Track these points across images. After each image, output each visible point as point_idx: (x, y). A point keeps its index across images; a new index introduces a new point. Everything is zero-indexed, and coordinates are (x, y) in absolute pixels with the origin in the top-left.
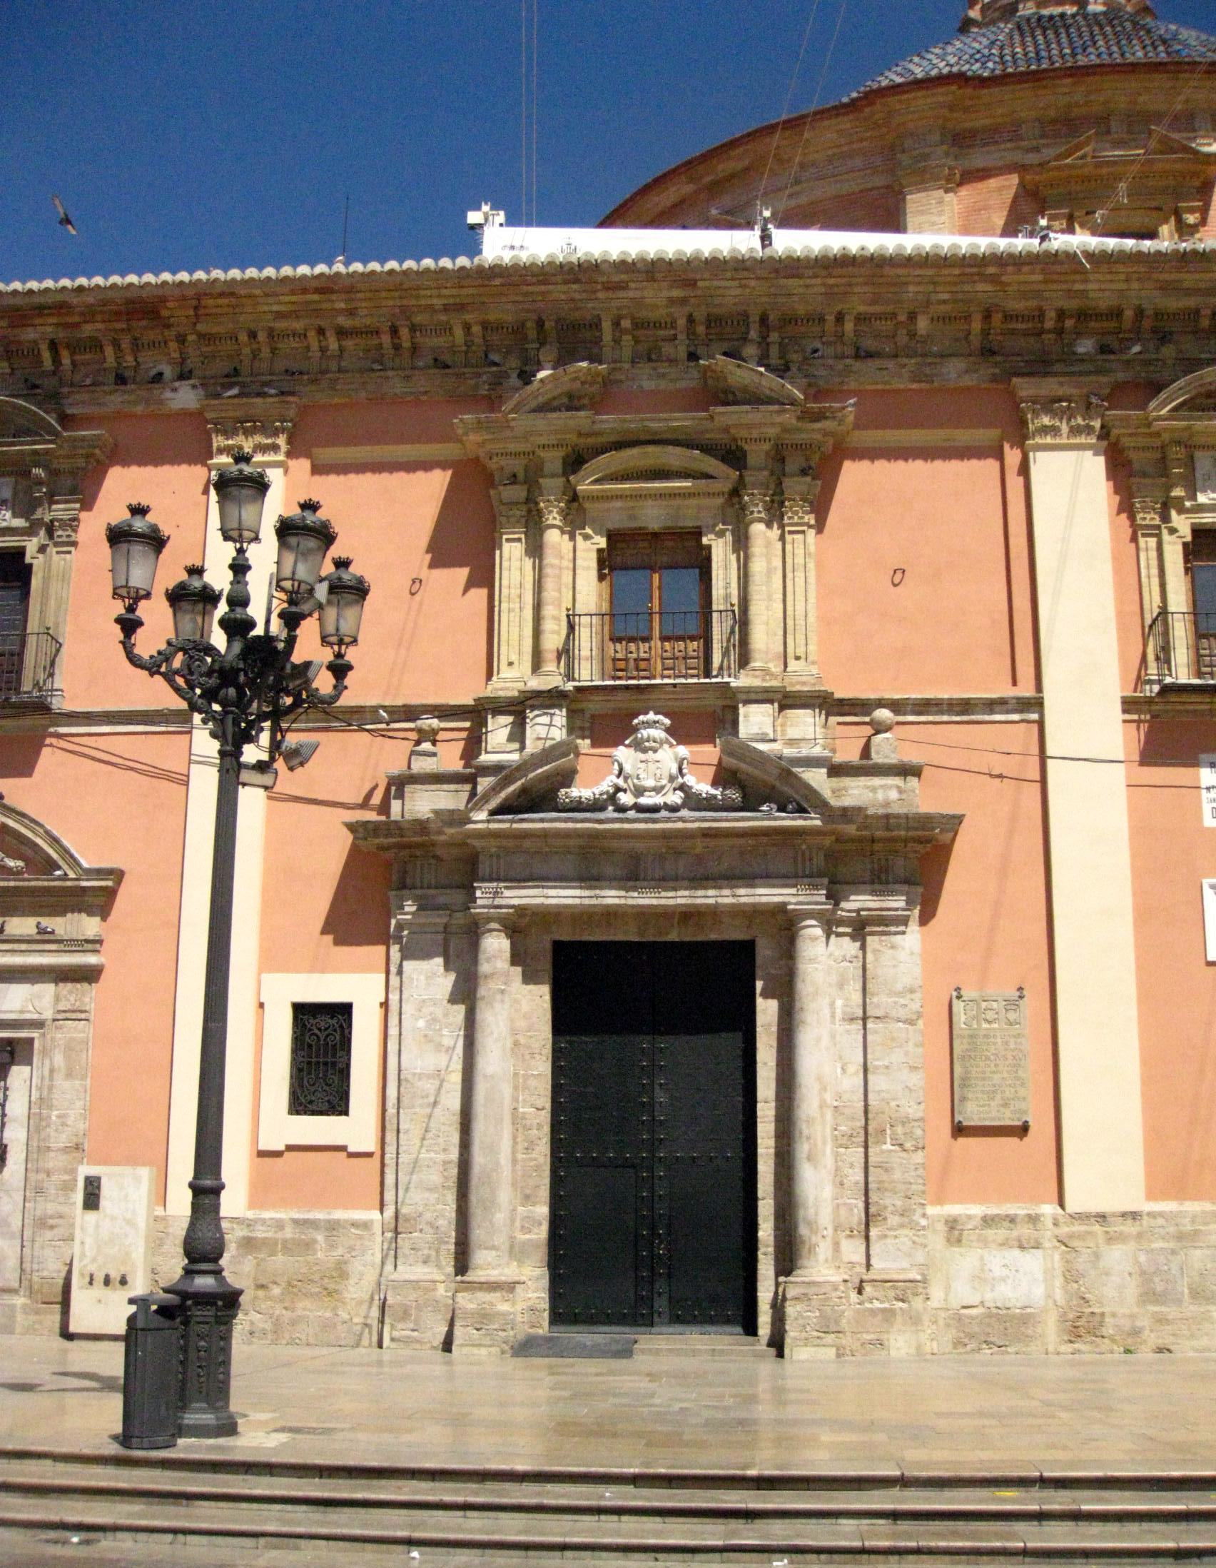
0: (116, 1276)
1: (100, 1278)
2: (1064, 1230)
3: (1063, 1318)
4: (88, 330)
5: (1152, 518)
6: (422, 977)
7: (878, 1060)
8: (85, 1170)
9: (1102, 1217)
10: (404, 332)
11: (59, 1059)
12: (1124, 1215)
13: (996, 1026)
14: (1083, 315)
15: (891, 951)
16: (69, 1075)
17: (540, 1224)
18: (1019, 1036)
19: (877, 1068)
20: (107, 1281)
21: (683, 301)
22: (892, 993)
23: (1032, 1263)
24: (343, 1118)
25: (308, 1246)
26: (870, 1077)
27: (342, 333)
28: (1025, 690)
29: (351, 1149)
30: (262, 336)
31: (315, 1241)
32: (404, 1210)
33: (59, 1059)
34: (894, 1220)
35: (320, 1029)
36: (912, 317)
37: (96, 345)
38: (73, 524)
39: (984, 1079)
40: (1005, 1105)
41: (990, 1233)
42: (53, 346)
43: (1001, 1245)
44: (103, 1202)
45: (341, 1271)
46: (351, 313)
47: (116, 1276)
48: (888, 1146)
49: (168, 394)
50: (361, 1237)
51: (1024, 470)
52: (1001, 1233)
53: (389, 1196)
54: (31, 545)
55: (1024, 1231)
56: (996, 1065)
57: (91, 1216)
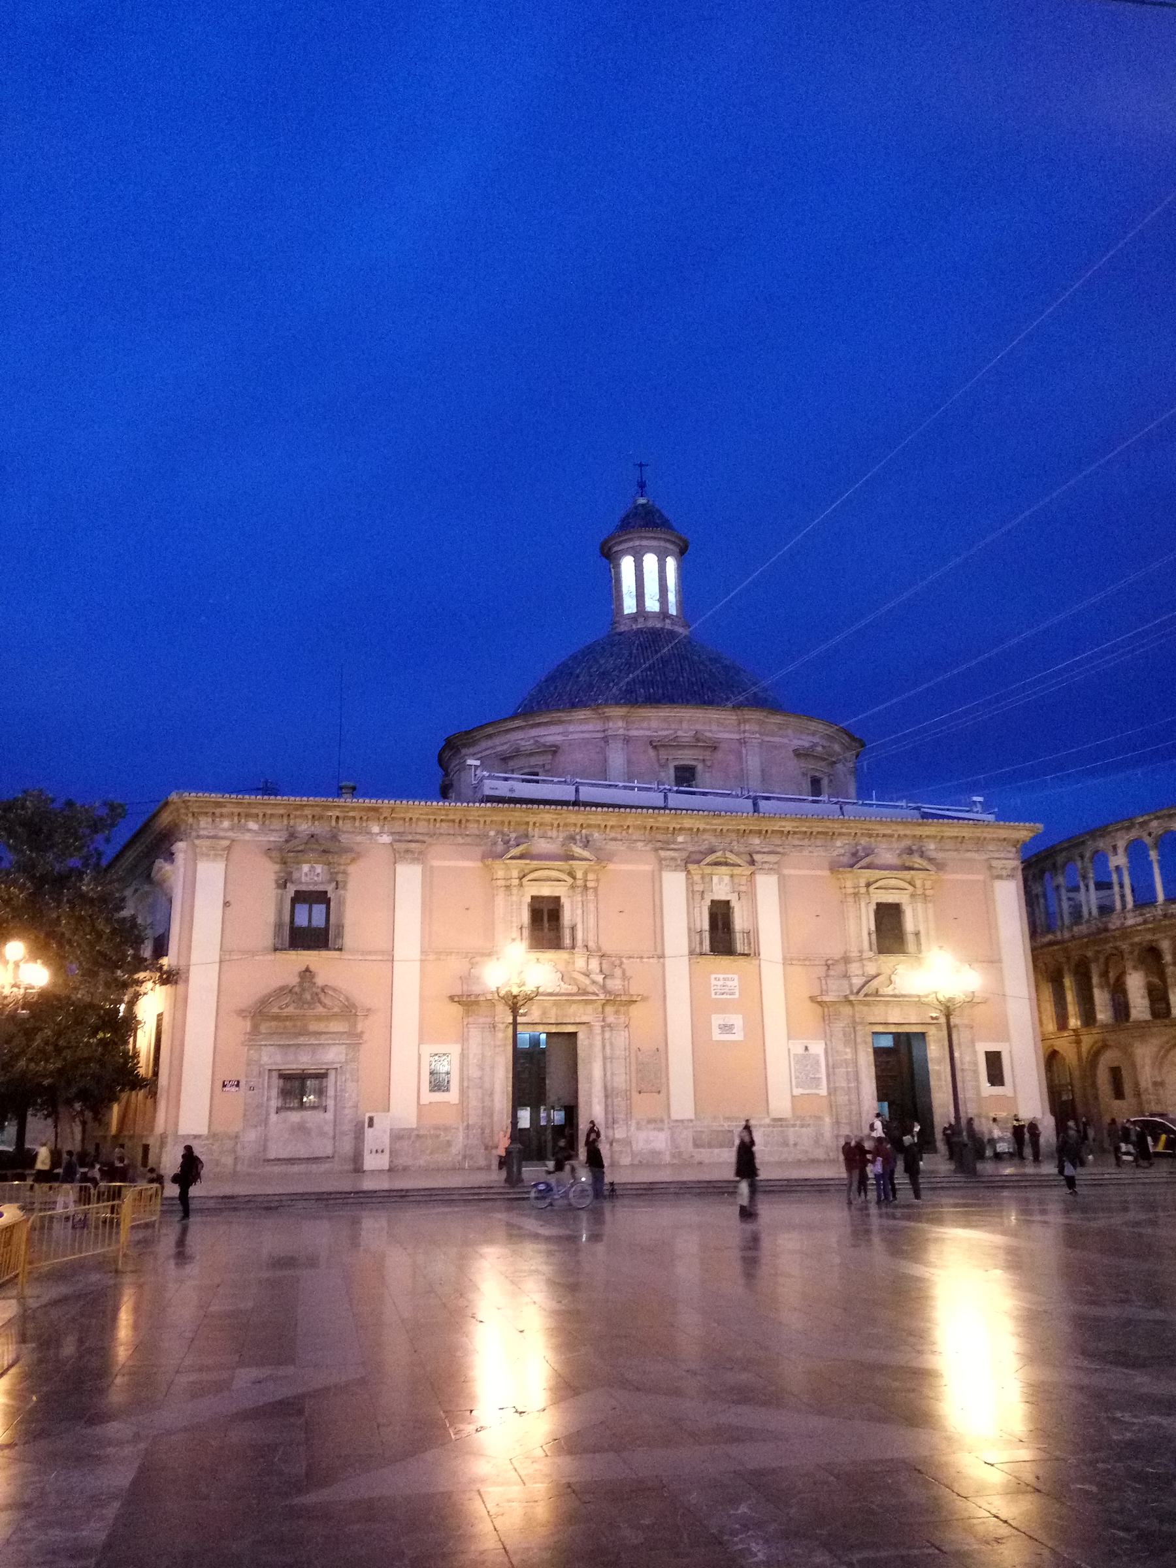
0: (380, 1151)
1: (374, 1150)
2: (672, 1124)
3: (671, 1153)
4: (351, 814)
5: (698, 897)
8: (368, 1115)
9: (682, 1121)
10: (463, 822)
11: (348, 1076)
12: (688, 1120)
14: (681, 829)
16: (352, 1081)
20: (377, 1151)
21: (557, 819)
25: (438, 1136)
27: (442, 821)
28: (659, 952)
30: (414, 820)
33: (348, 1076)
36: (628, 827)
37: (354, 818)
38: (345, 883)
41: (650, 1126)
42: (338, 817)
45: (449, 1144)
46: (447, 815)
47: (380, 1151)
49: (378, 838)
51: (661, 878)
52: (653, 1126)
54: (330, 888)
55: (659, 1125)
57: (371, 1130)
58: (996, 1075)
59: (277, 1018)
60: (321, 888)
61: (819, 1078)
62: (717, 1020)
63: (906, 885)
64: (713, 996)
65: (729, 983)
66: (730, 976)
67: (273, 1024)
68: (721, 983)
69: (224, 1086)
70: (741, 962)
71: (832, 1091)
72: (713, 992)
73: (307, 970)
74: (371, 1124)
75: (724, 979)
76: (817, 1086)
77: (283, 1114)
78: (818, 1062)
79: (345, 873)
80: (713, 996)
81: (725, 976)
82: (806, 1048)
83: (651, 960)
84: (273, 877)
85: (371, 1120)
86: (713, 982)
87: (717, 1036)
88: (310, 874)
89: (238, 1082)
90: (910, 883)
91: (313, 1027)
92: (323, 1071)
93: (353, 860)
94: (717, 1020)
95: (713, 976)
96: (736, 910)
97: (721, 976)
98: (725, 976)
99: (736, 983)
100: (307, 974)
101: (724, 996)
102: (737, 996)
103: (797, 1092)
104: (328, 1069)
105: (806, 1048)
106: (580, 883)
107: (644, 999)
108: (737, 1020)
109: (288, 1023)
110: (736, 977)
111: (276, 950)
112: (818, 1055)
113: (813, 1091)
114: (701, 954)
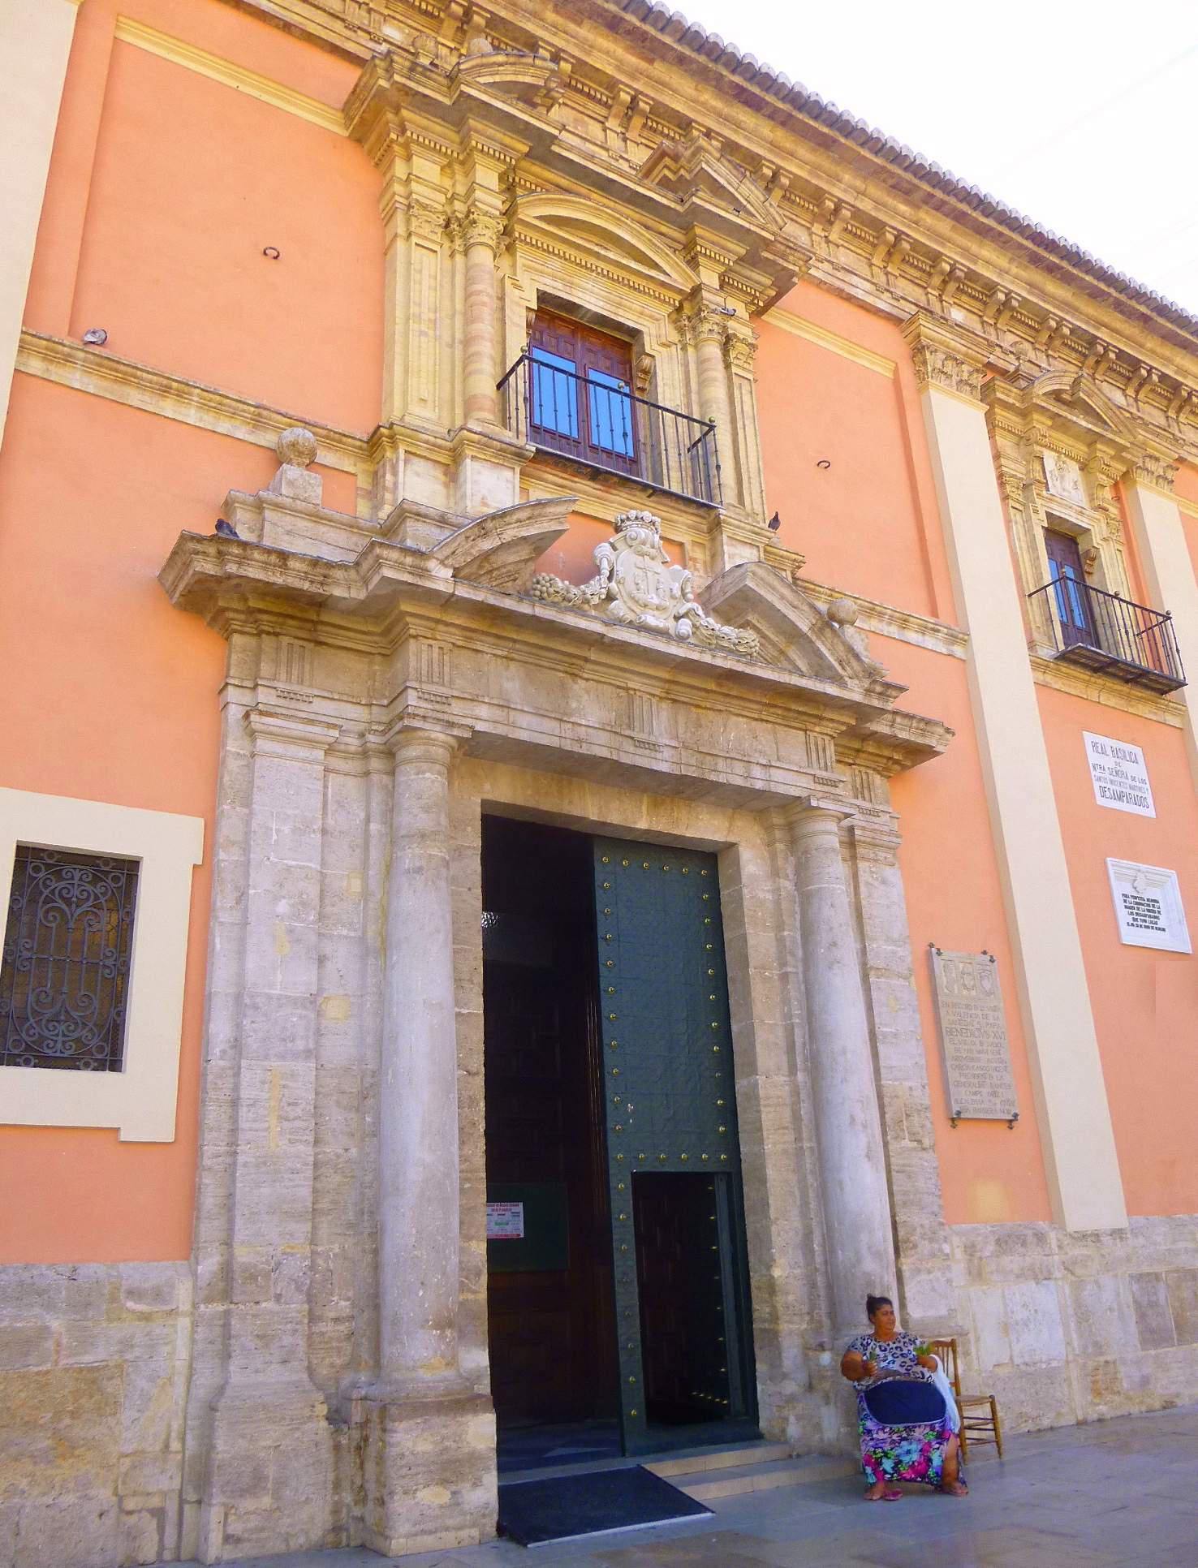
6: (286, 829)
7: (886, 1025)
9: (1096, 1236)
13: (973, 993)
15: (882, 887)
17: (478, 1274)
18: (995, 1009)
19: (885, 1035)
22: (889, 940)
23: (1049, 1299)
24: (108, 1075)
26: (882, 1049)
29: (124, 1136)
31: (44, 1332)
32: (243, 1255)
34: (925, 1247)
35: (68, 902)
39: (972, 1059)
40: (994, 1094)
43: (1018, 1276)
48: (906, 1143)
50: (146, 1317)
53: (210, 1230)
55: (1034, 1256)
56: (981, 1044)
72: (1096, 785)
80: (1101, 801)
83: (930, 642)
97: (1109, 742)
99: (1139, 770)
102: (1151, 813)
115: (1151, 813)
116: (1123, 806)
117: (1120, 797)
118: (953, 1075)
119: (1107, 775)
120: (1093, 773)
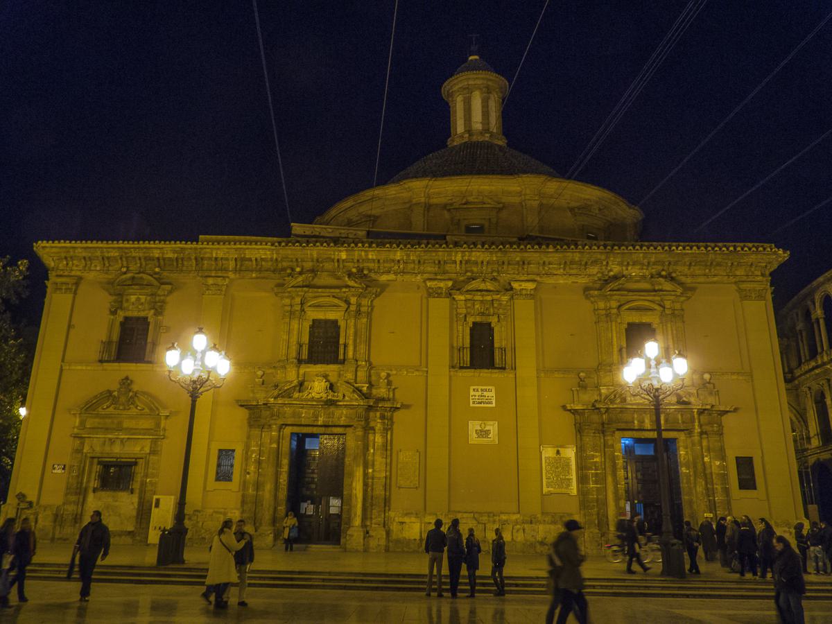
44: (160, 506)
57: (157, 510)
58: (748, 482)
59: (98, 416)
60: (142, 314)
61: (569, 479)
62: (474, 426)
63: (657, 307)
64: (471, 405)
65: (485, 393)
66: (488, 388)
67: (97, 420)
68: (480, 393)
69: (54, 469)
70: (495, 375)
71: (583, 493)
72: (471, 401)
73: (127, 378)
74: (157, 505)
75: (482, 390)
76: (568, 485)
77: (100, 494)
78: (568, 465)
79: (163, 302)
80: (471, 405)
81: (483, 388)
82: (558, 452)
84: (108, 305)
85: (158, 500)
86: (472, 393)
87: (474, 438)
88: (136, 305)
89: (64, 466)
90: (660, 305)
91: (126, 424)
92: (134, 460)
93: (170, 292)
94: (474, 426)
95: (472, 388)
96: (496, 330)
97: (480, 388)
98: (483, 388)
99: (493, 394)
100: (126, 382)
101: (482, 405)
102: (494, 405)
103: (545, 490)
104: (136, 459)
105: (558, 452)
106: (353, 308)
107: (407, 407)
108: (493, 427)
109: (107, 420)
110: (493, 389)
111: (101, 361)
112: (569, 459)
113: (564, 491)
114: (461, 368)
115: (494, 405)
116: (482, 405)
117: (481, 403)
118: (399, 478)
119: (477, 397)
120: (471, 397)
